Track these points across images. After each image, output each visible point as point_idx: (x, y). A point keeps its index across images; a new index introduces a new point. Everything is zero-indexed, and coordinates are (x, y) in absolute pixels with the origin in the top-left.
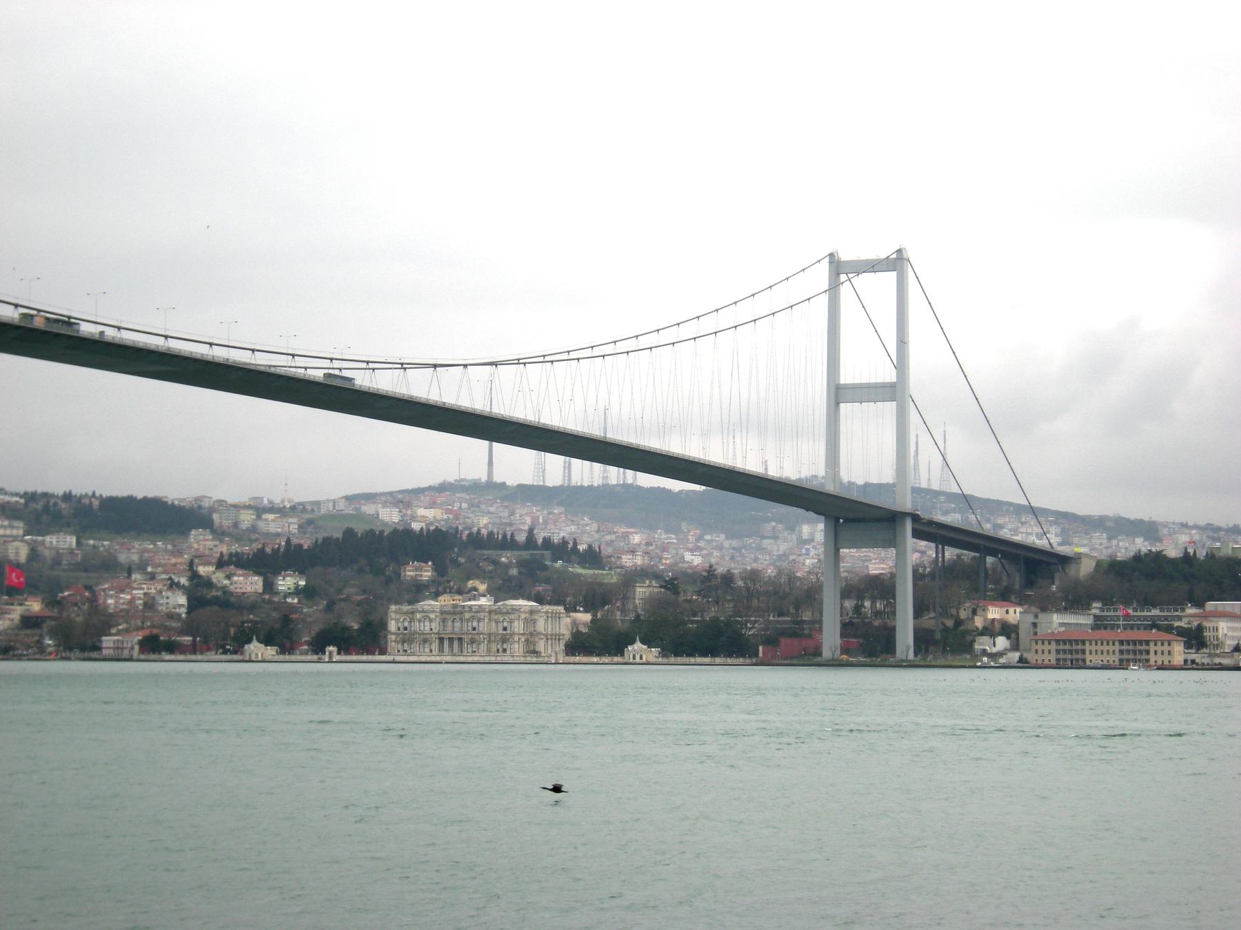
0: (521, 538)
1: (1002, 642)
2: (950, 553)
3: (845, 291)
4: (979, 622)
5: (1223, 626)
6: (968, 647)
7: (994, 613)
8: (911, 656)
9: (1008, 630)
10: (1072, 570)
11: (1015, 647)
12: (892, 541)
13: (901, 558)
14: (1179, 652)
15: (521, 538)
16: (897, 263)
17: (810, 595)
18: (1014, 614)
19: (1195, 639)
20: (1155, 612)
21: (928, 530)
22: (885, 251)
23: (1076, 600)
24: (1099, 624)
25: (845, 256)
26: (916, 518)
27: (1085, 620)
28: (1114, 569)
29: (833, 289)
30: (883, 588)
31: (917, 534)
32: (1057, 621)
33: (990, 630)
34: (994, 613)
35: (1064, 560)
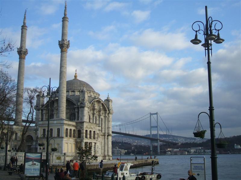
0: (122, 142)
1: (169, 152)
2: (164, 143)
3: (152, 116)
4: (167, 150)
5: (192, 150)
6: (166, 153)
7: (169, 149)
8: (159, 154)
9: (170, 151)
10: (178, 144)
11: (171, 153)
12: (157, 142)
13: (158, 144)
14: (186, 153)
15: (122, 142)
16: (156, 114)
17: (149, 147)
18: (171, 149)
19: (188, 152)
20: (185, 149)
21: (161, 141)
22: (155, 112)
23: (177, 148)
24: (180, 150)
25: (152, 113)
26: (160, 140)
27: (178, 150)
28: (182, 144)
29: (150, 116)
30: (156, 147)
31: (160, 141)
32: (175, 150)
33: (168, 151)
34: (169, 149)
35: (177, 143)
